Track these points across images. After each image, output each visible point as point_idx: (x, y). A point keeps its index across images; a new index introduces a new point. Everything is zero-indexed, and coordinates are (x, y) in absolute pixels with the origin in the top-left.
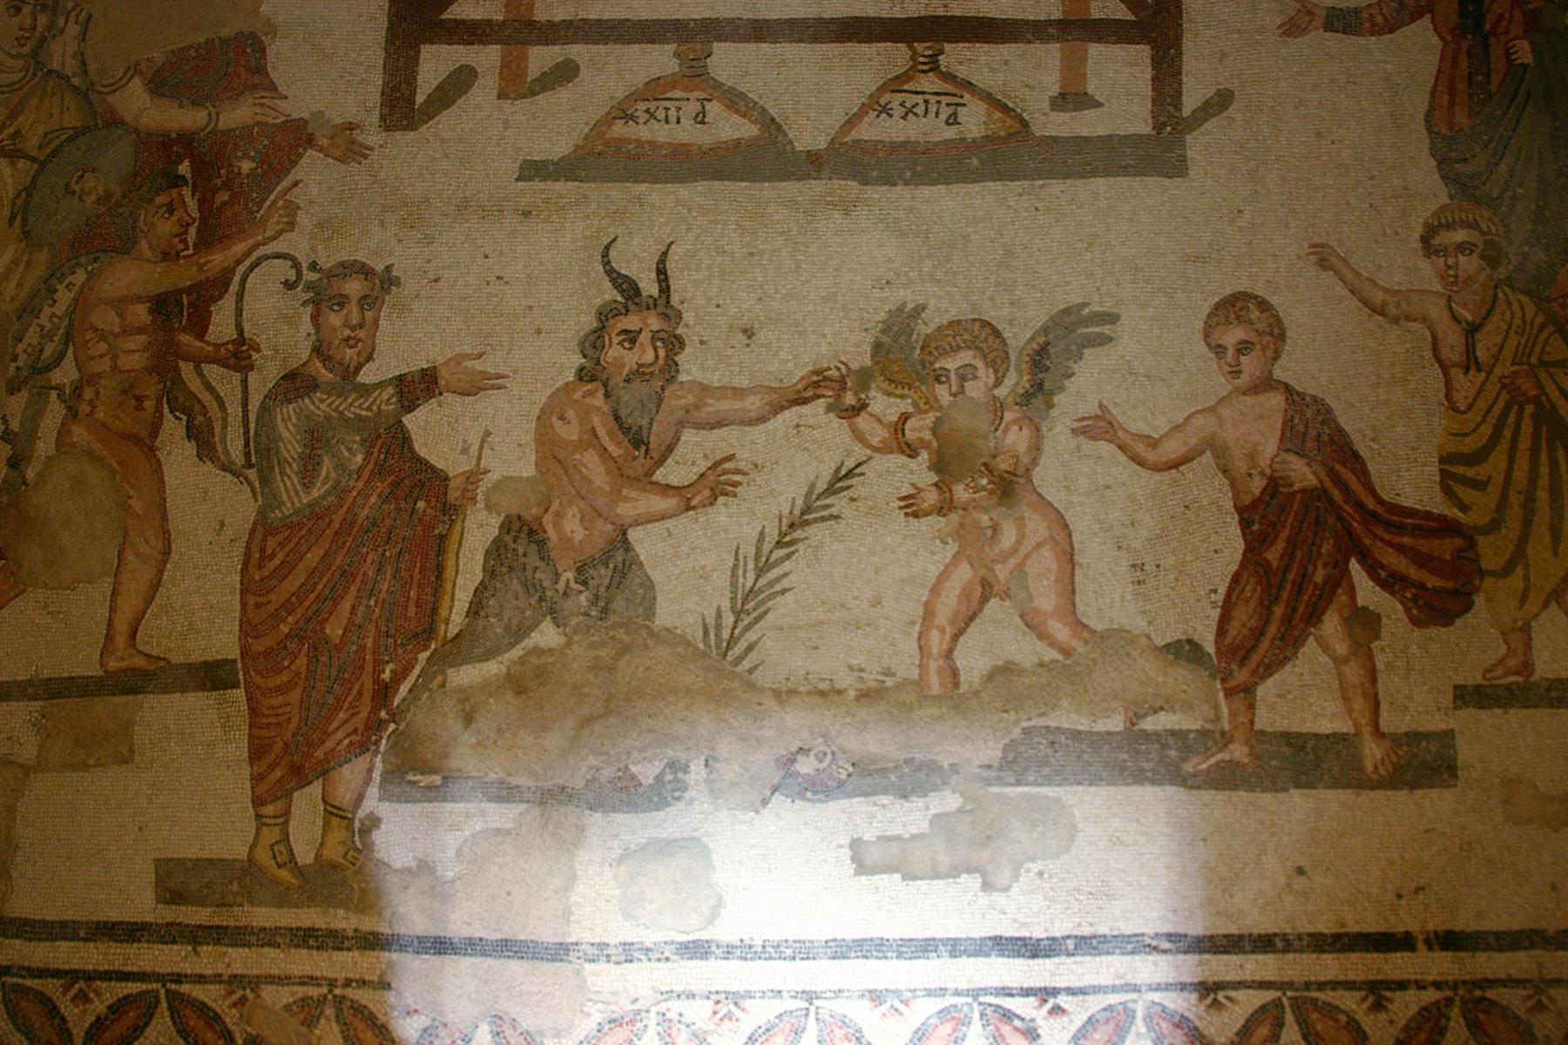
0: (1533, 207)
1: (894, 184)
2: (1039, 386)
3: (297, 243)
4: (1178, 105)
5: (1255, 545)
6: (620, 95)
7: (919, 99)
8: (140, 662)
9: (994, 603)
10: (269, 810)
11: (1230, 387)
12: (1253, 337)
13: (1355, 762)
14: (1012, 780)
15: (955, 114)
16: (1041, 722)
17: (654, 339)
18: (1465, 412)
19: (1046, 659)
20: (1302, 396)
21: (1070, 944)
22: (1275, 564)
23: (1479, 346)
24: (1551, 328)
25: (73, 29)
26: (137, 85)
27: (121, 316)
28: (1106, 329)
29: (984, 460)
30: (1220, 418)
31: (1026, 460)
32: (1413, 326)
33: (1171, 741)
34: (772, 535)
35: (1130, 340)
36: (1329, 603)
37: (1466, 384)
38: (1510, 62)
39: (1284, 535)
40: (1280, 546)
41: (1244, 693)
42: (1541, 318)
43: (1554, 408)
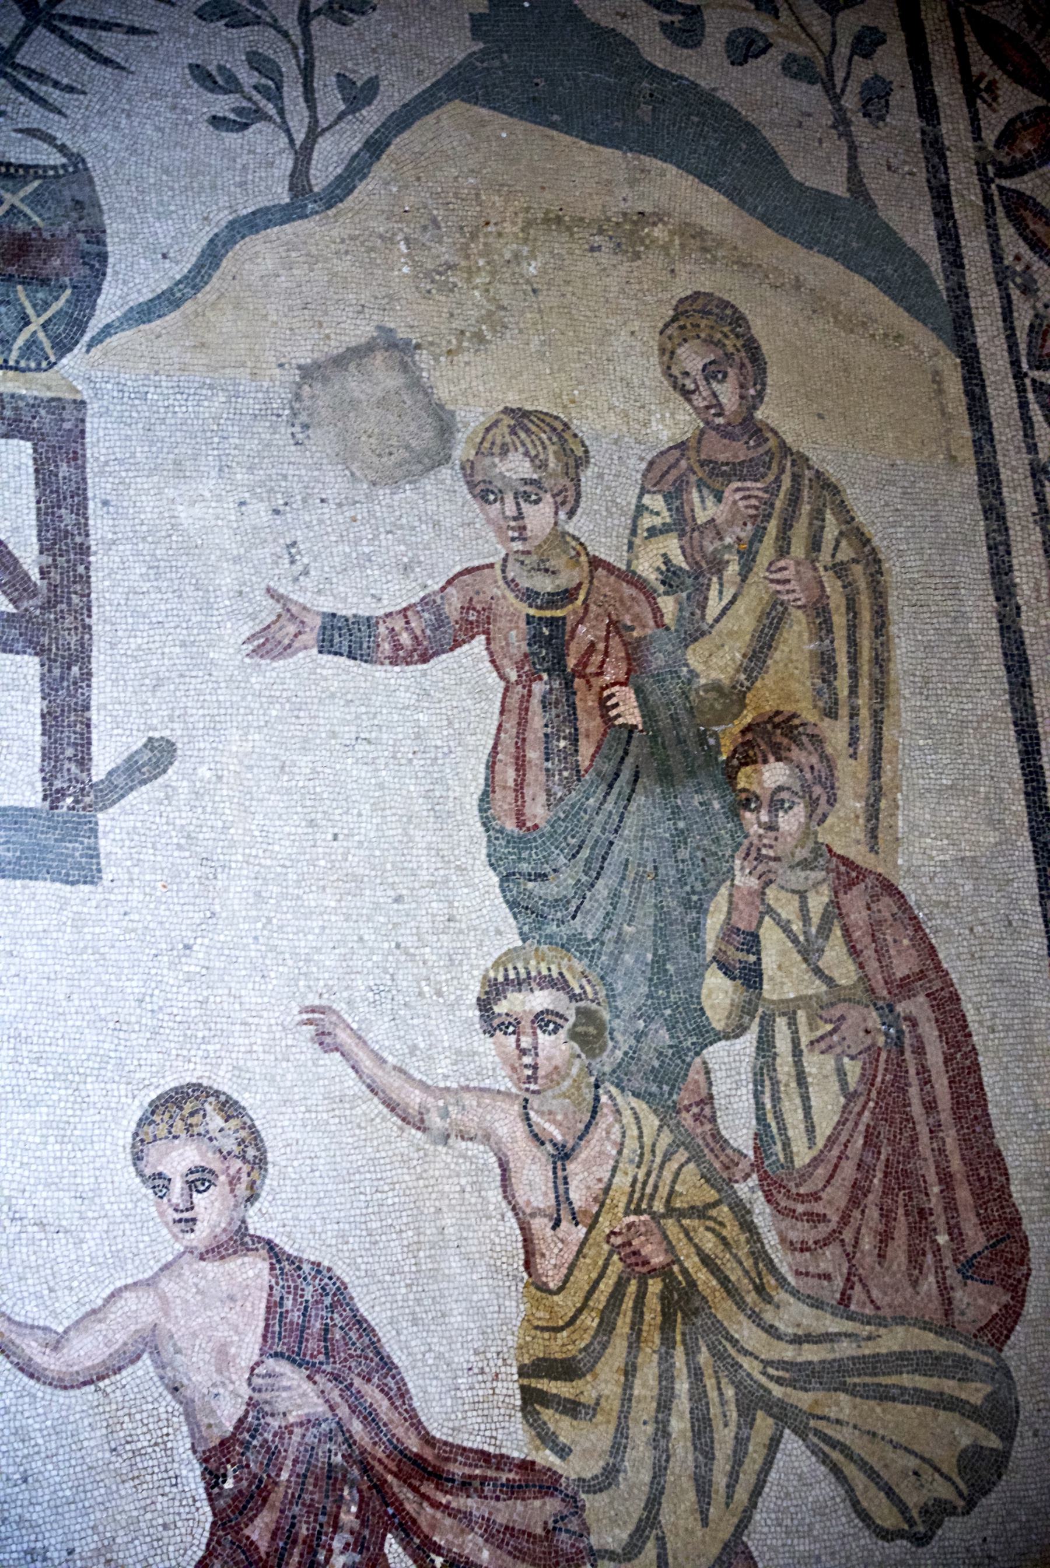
0: (649, 957)
4: (84, 761)
11: (179, 1247)
18: (551, 1293)
20: (296, 1263)
22: (263, 1546)
23: (573, 1184)
24: (682, 1155)
30: (164, 1299)
32: (475, 1149)
38: (608, 721)
42: (666, 1139)
43: (692, 1284)
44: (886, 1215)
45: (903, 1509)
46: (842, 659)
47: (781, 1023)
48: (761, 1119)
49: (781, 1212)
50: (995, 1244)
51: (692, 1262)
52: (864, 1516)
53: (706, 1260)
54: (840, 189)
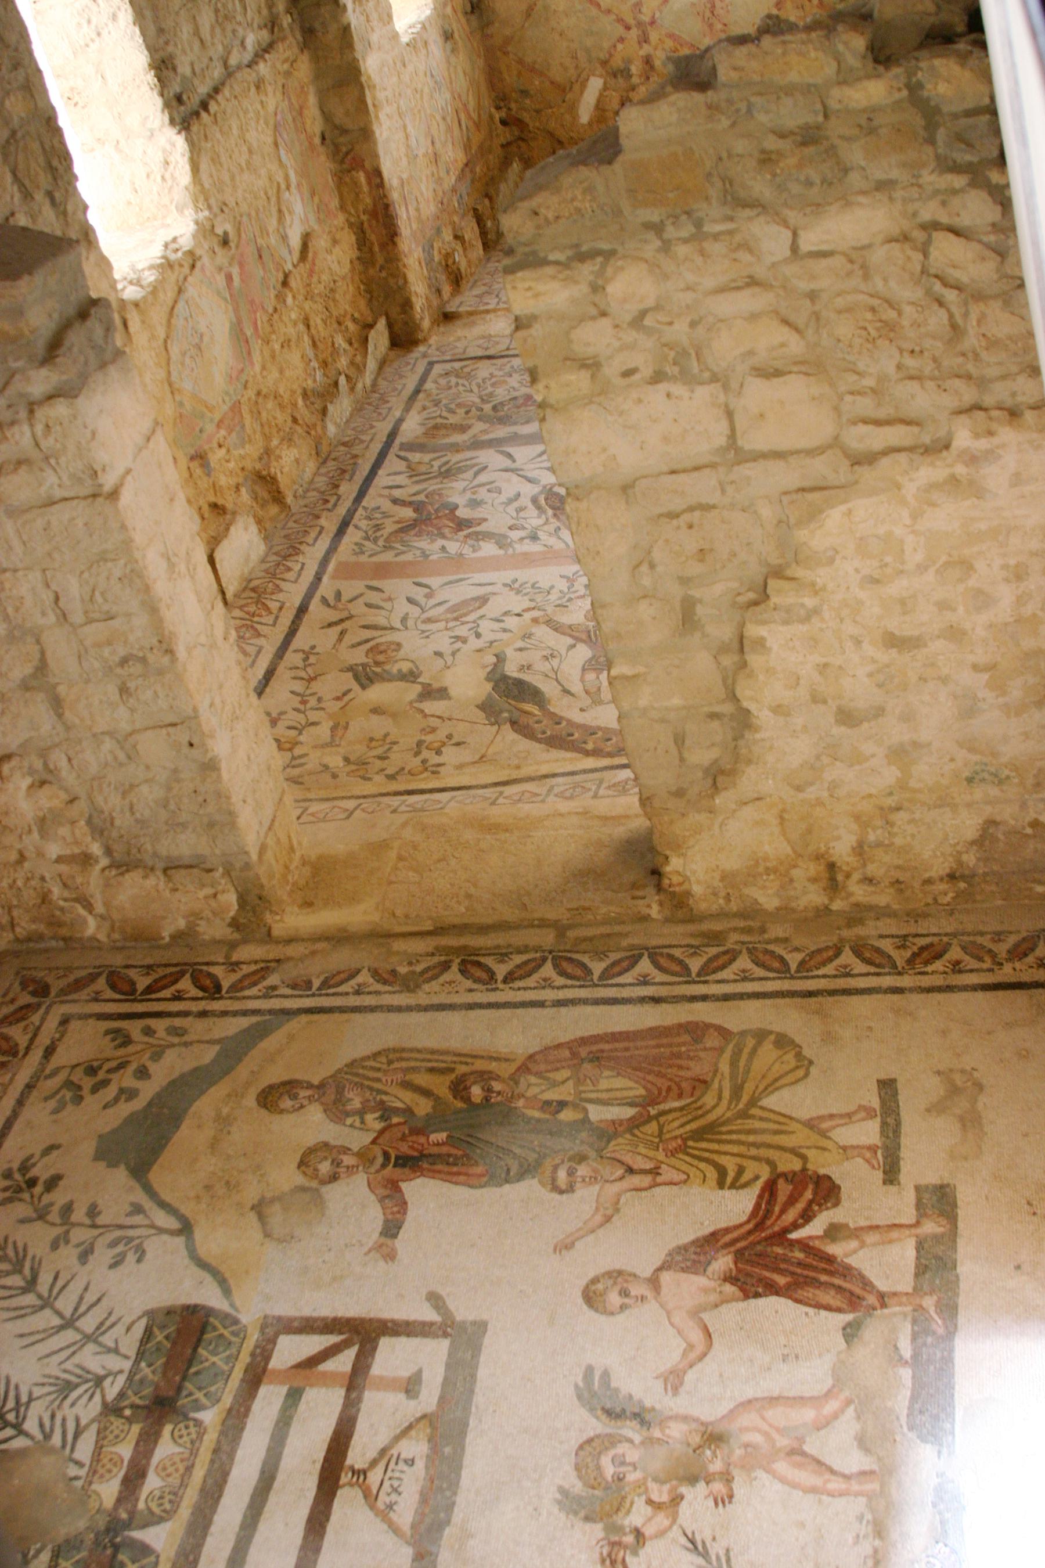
1: (454, 1503)
2: (636, 1415)
4: (432, 1324)
5: (772, 1289)
7: (387, 1484)
9: (806, 1448)
13: (937, 1238)
14: (950, 1438)
15: (406, 1461)
16: (903, 1420)
19: (853, 1415)
22: (789, 1279)
29: (691, 1451)
31: (694, 1426)
32: (623, 1200)
33: (920, 1341)
36: (819, 1250)
37: (668, 1173)
38: (443, 1144)
39: (768, 1274)
41: (883, 1299)
42: (628, 1136)
44: (670, 1066)
45: (797, 1067)
47: (583, 1095)
49: (665, 1100)
50: (687, 1031)
51: (682, 1131)
53: (682, 1126)
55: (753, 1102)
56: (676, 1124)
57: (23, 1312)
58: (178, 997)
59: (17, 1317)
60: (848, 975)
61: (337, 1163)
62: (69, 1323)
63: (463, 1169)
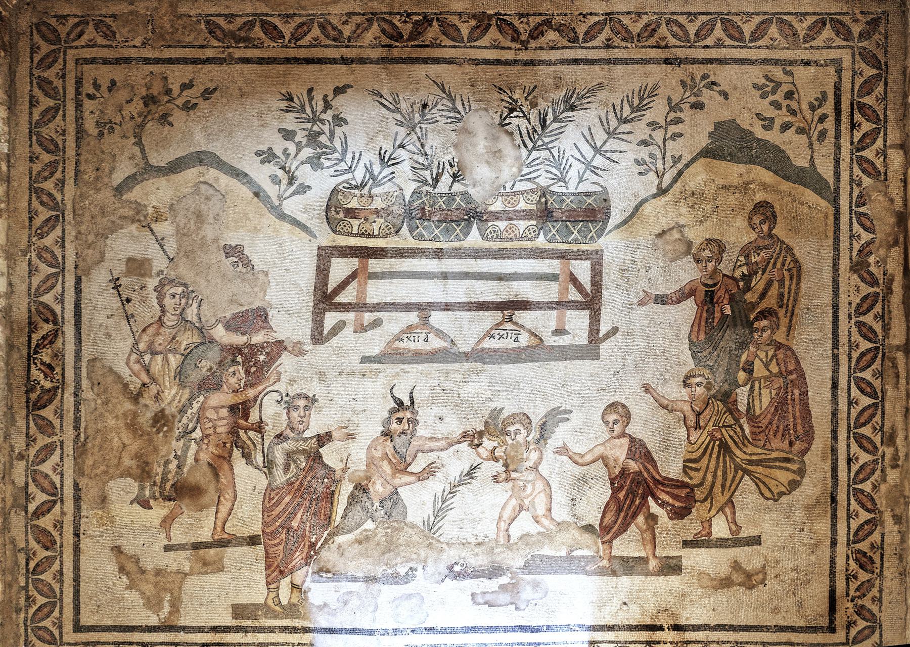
3: (281, 386)
5: (615, 491)
6: (398, 331)
7: (505, 332)
8: (226, 536)
9: (524, 512)
10: (272, 586)
12: (619, 418)
17: (408, 421)
21: (545, 628)
25: (195, 305)
26: (220, 327)
27: (217, 413)
28: (567, 416)
34: (448, 489)
35: (576, 418)
38: (722, 314)
40: (624, 492)
46: (786, 293)
47: (757, 382)
48: (748, 404)
50: (806, 433)
51: (727, 437)
52: (762, 494)
53: (730, 437)
54: (807, 165)
55: (746, 472)
56: (732, 433)
57: (605, 124)
58: (853, 126)
59: (601, 122)
60: (849, 517)
61: (709, 260)
62: (597, 150)
63: (703, 328)
